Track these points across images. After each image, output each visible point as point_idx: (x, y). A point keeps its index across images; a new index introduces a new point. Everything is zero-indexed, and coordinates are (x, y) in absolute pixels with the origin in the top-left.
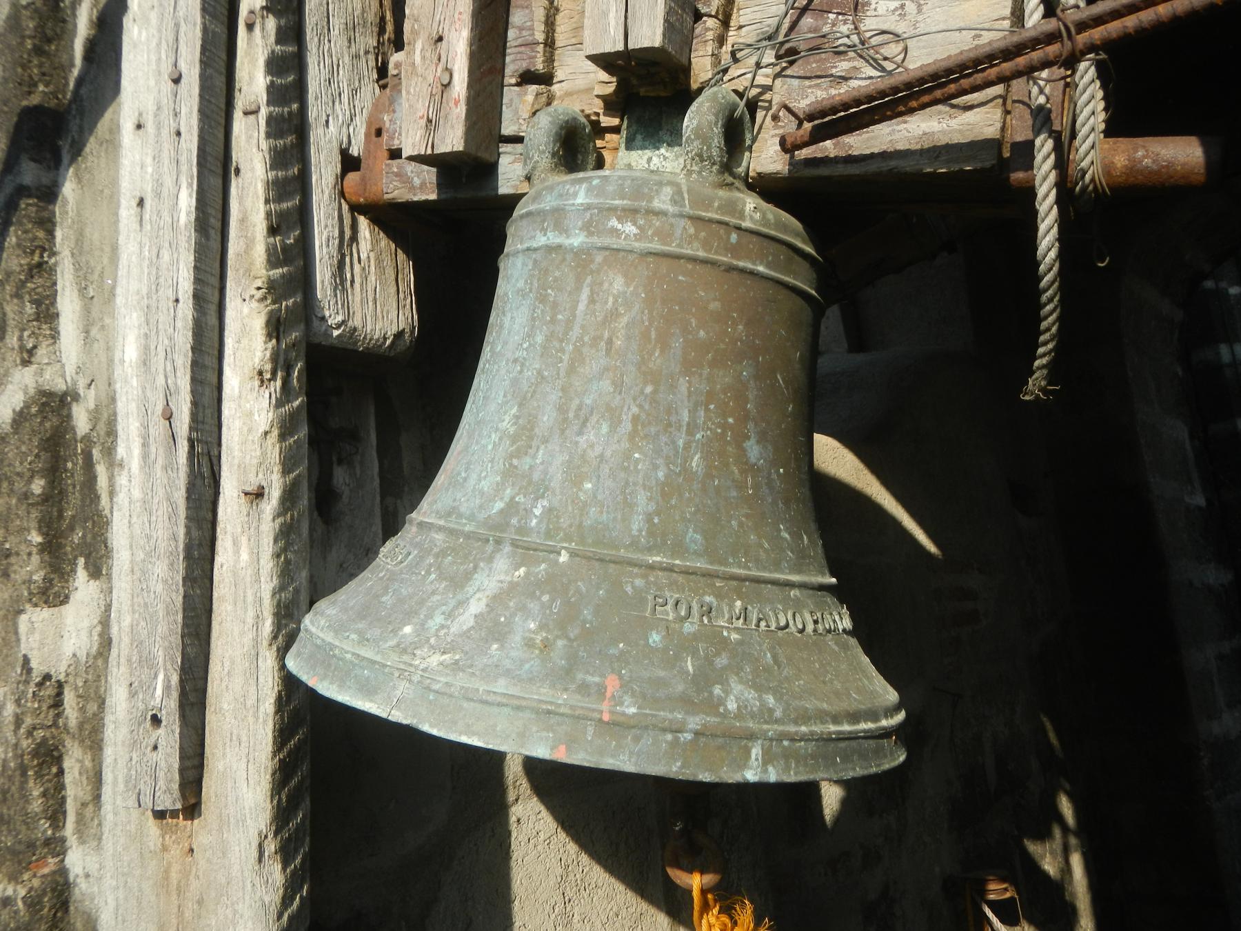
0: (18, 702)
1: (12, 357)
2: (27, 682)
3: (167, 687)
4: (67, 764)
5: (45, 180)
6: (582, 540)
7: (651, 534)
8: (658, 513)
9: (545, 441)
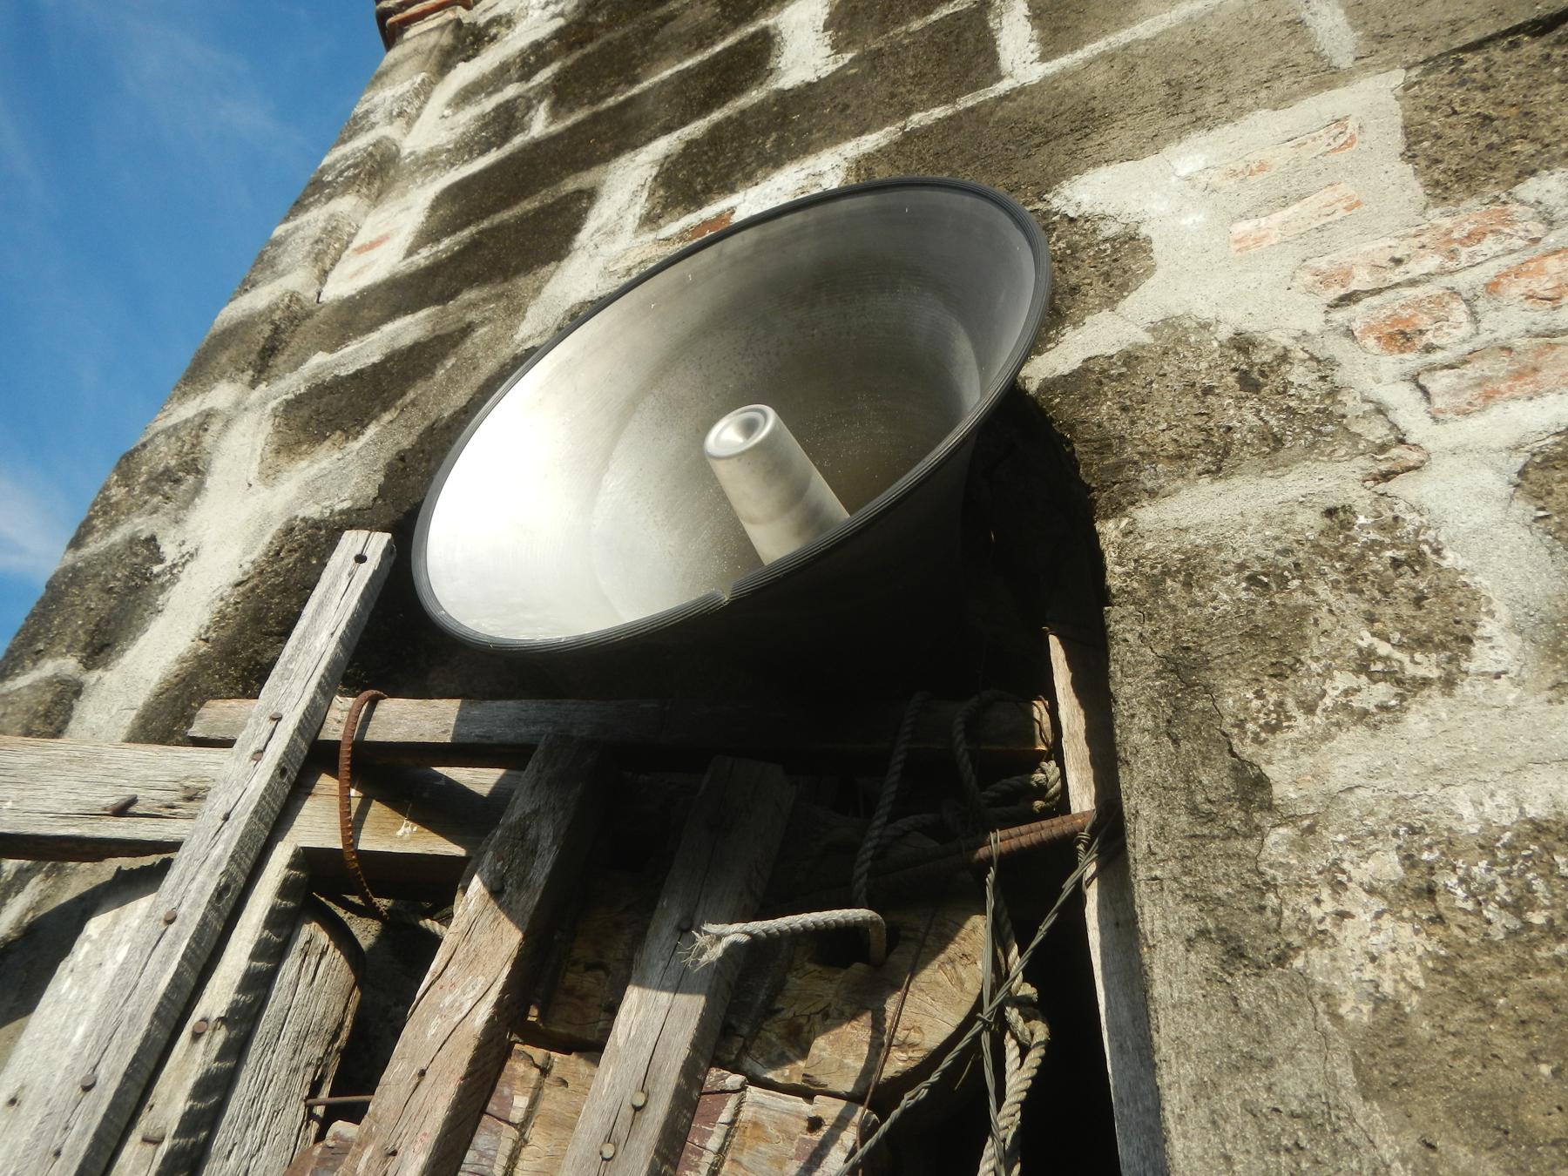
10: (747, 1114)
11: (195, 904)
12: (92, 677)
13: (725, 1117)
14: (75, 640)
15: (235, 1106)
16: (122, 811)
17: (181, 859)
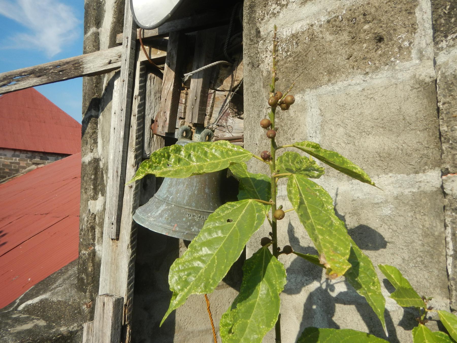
0: (88, 218)
1: (88, 150)
2: (89, 214)
3: (115, 218)
4: (96, 230)
5: (96, 114)
6: (176, 203)
7: (187, 203)
8: (188, 200)
9: (173, 186)
10: (216, 96)
11: (126, 78)
13: (212, 97)
14: (93, 23)
15: (147, 108)
16: (110, 63)
17: (121, 69)
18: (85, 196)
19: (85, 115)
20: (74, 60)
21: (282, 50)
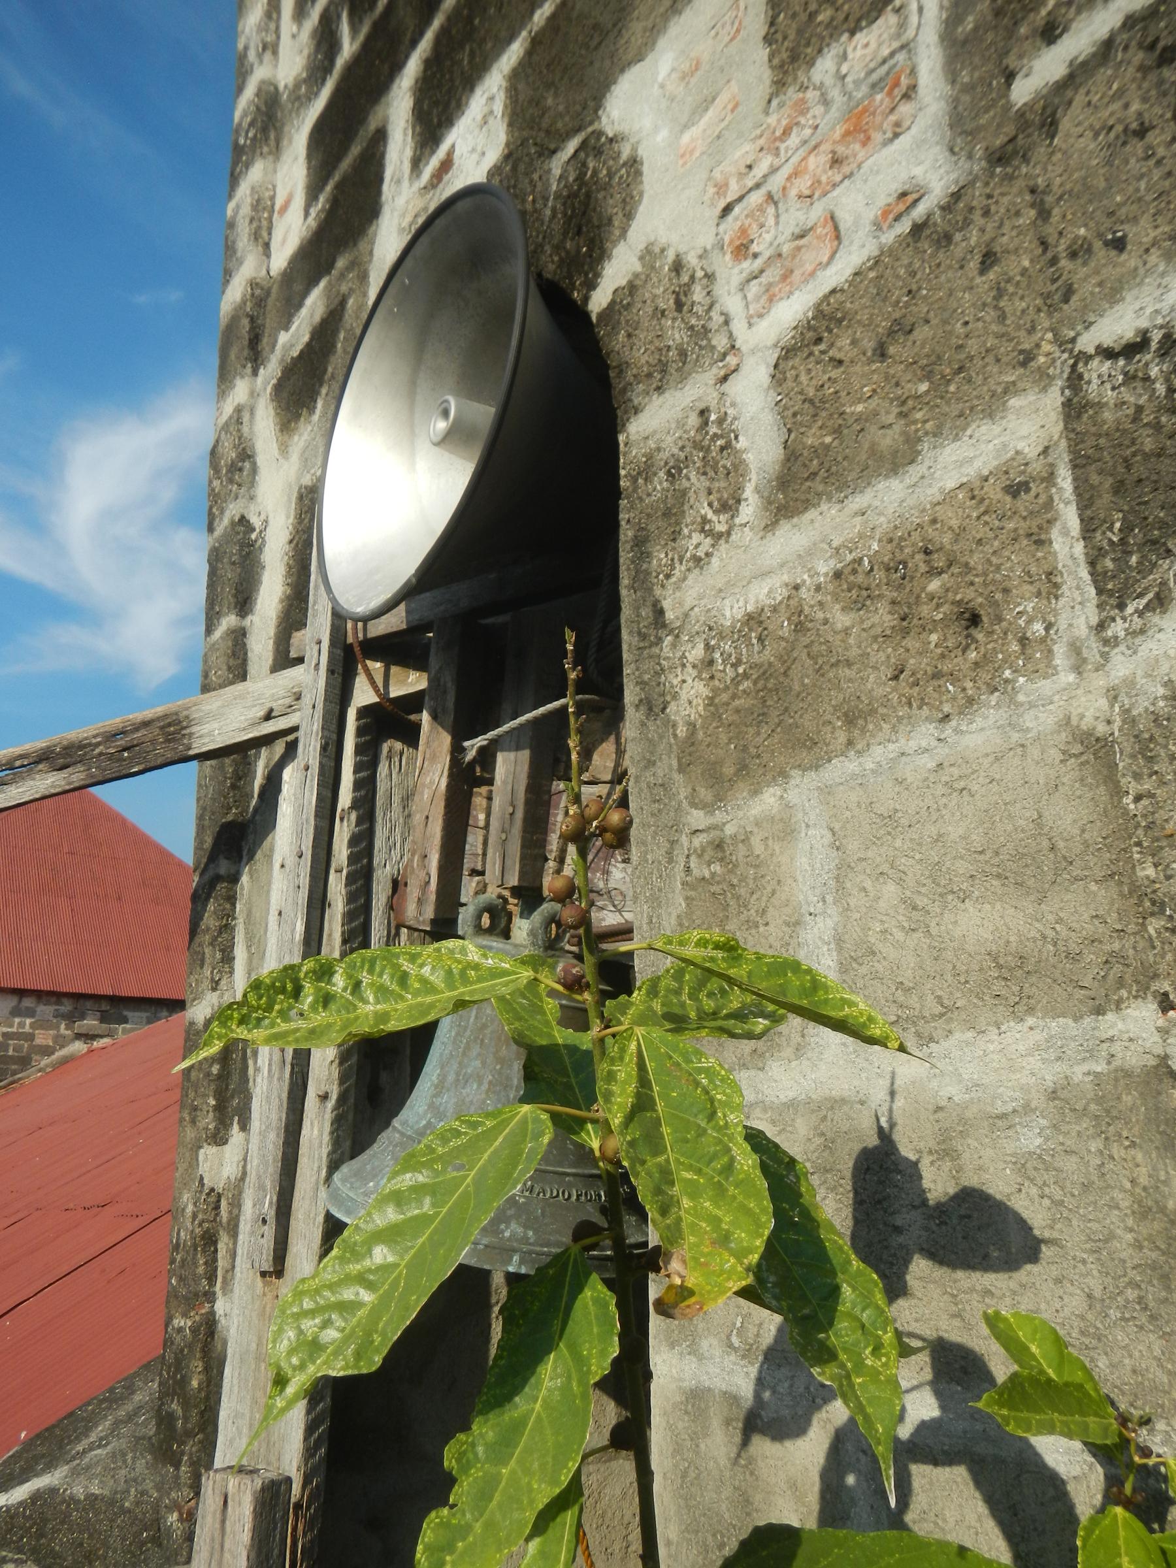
0: (195, 1204)
1: (206, 984)
2: (201, 1192)
3: (271, 1203)
4: (219, 1246)
5: (232, 871)
9: (448, 1090)
11: (314, 758)
12: (247, 622)
14: (229, 604)
16: (268, 717)
17: (301, 734)
18: (190, 1134)
19: (201, 875)
20: (166, 716)
21: (724, 661)
